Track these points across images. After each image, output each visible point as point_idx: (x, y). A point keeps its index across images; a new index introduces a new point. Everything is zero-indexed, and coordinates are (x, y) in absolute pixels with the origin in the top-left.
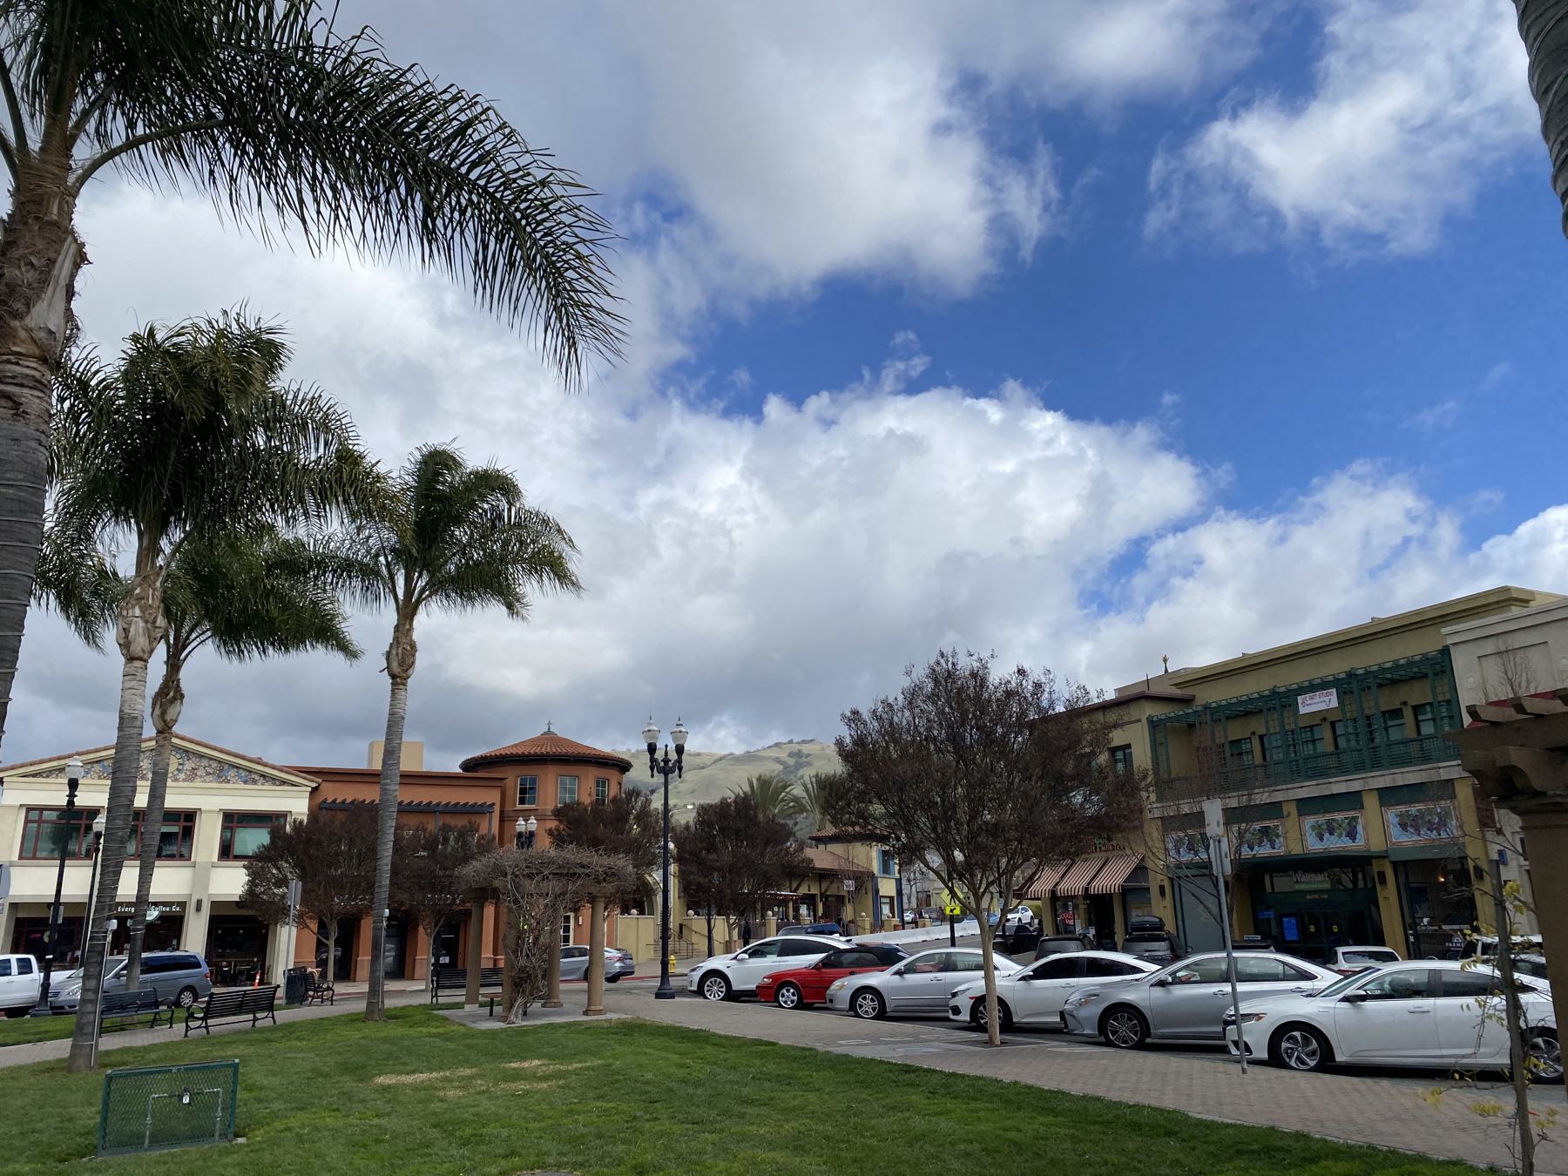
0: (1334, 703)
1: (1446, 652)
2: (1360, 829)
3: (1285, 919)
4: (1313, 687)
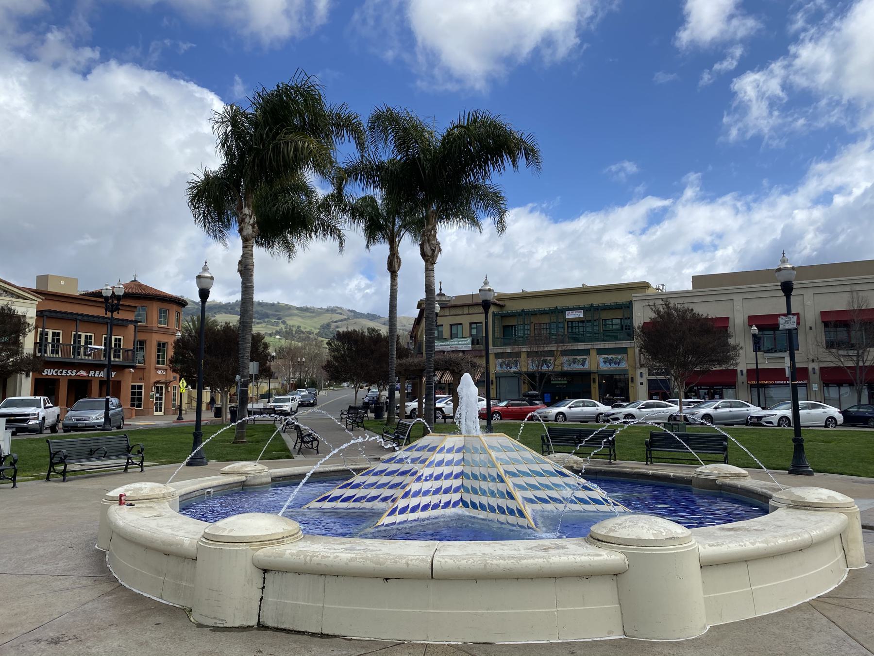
0: (582, 315)
1: (631, 302)
2: (587, 362)
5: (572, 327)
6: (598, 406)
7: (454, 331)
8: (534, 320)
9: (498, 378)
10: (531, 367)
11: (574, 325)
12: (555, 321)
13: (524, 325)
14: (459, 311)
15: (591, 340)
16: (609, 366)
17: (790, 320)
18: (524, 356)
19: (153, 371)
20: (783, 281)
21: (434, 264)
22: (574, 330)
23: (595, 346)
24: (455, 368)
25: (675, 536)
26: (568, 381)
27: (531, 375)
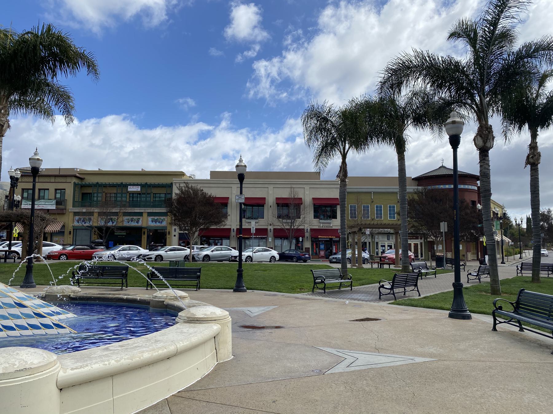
1: (172, 184)
2: (140, 221)
3: (110, 242)
4: (134, 185)
5: (133, 197)
6: (140, 250)
7: (42, 194)
8: (104, 190)
9: (75, 230)
10: (102, 223)
11: (134, 196)
12: (120, 192)
13: (98, 193)
14: (46, 179)
15: (145, 206)
16: (155, 224)
17: (241, 197)
18: (96, 215)
20: (239, 173)
21: (3, 136)
22: (134, 199)
23: (146, 210)
24: (26, 221)
25: (27, 367)
26: (126, 233)
27: (100, 229)
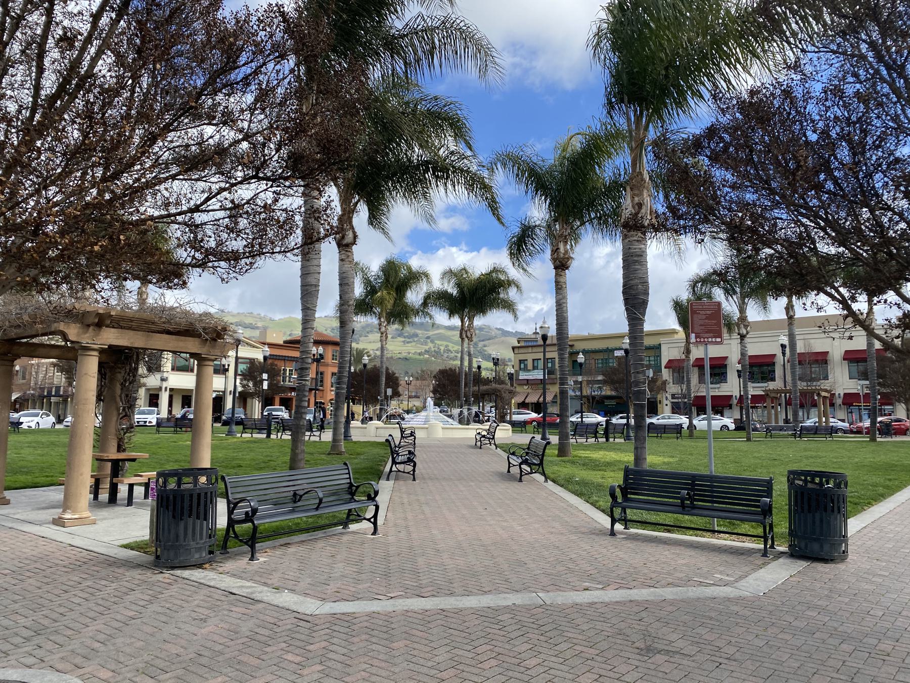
1: (660, 345)
7: (536, 365)
19: (329, 391)
